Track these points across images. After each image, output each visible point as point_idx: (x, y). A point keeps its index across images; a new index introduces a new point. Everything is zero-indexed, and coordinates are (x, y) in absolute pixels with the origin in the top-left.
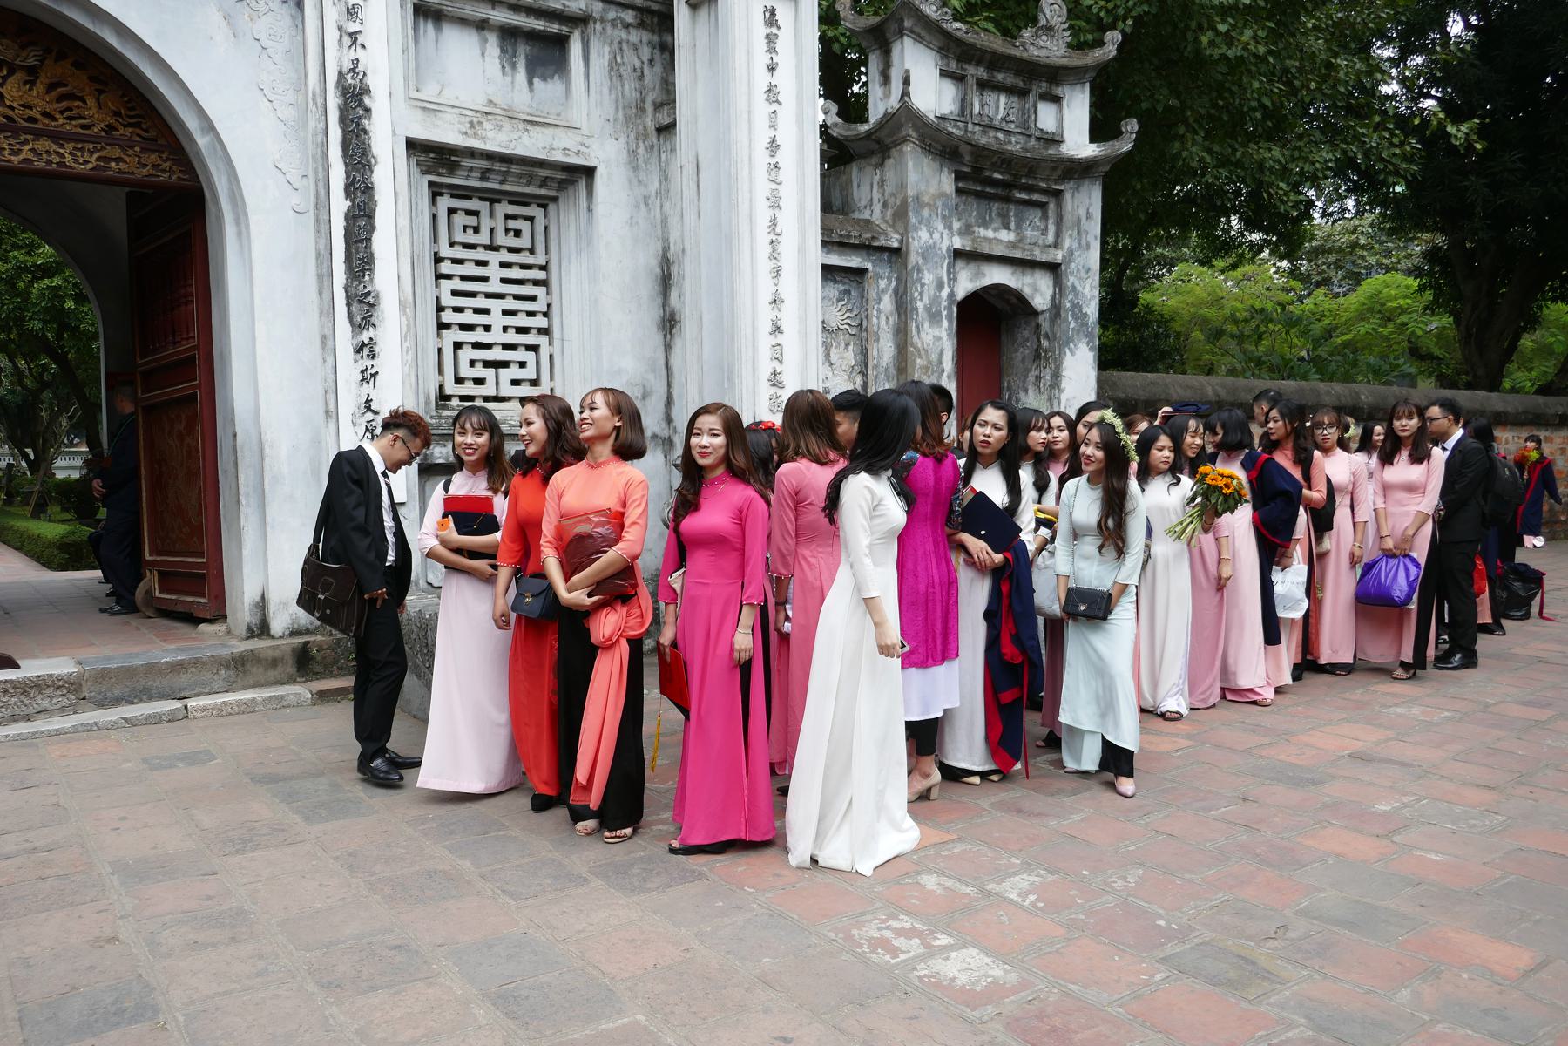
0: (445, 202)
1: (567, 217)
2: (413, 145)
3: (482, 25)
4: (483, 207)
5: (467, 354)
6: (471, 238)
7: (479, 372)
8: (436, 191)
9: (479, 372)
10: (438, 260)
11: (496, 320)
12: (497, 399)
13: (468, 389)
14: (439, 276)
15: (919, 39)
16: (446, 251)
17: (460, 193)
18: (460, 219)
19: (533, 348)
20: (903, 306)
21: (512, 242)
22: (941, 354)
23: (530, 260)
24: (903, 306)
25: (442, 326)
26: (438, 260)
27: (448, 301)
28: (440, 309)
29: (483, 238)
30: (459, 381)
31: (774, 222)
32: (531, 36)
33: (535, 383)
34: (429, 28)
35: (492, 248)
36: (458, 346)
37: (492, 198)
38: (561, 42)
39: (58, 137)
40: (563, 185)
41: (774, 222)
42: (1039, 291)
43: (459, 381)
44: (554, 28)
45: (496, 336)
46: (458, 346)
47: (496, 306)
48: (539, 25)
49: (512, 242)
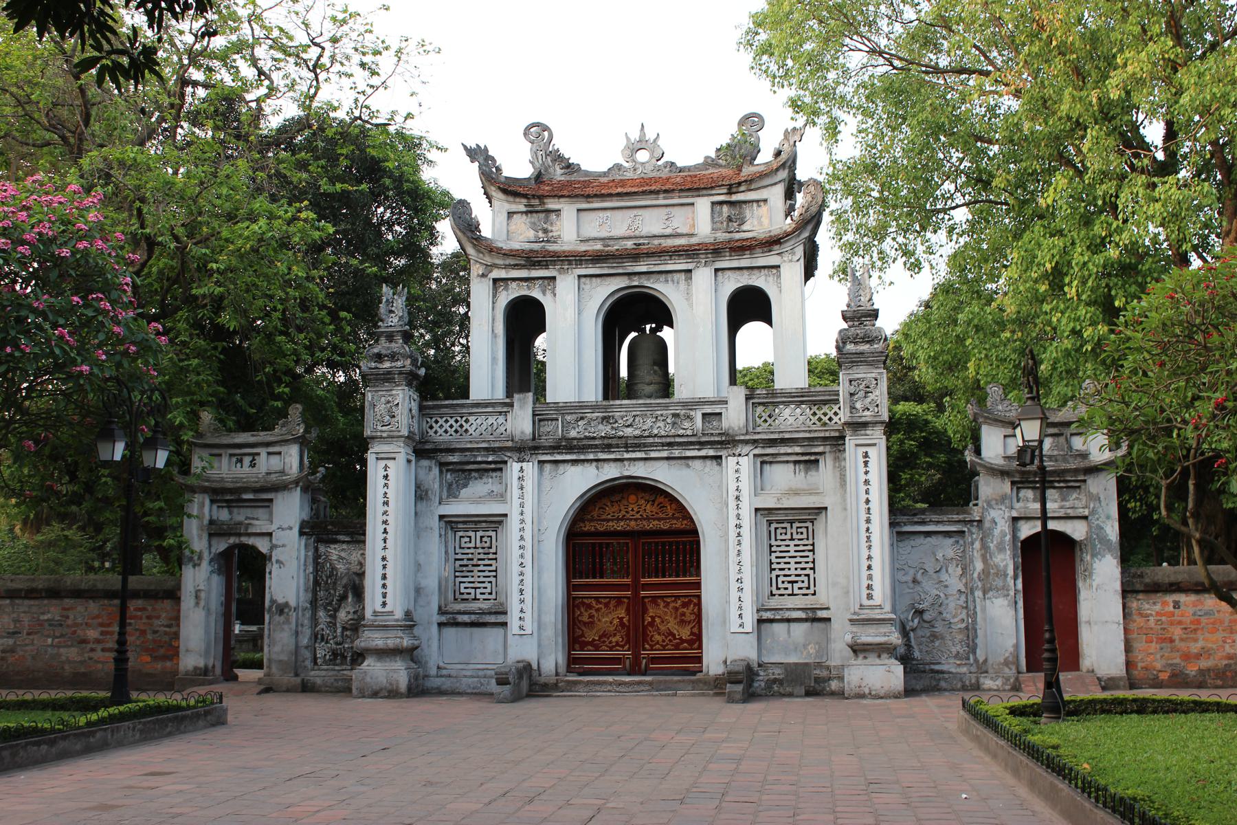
0: (774, 526)
1: (819, 525)
2: (757, 510)
3: (787, 462)
4: (788, 526)
5: (780, 580)
6: (783, 537)
7: (786, 585)
8: (770, 523)
9: (786, 585)
10: (771, 546)
11: (793, 566)
12: (793, 595)
13: (782, 591)
14: (771, 552)
15: (989, 424)
16: (773, 542)
17: (779, 522)
18: (779, 531)
19: (808, 575)
20: (984, 547)
21: (800, 536)
22: (1006, 566)
23: (805, 542)
24: (984, 547)
25: (772, 570)
26: (771, 546)
27: (774, 560)
28: (771, 563)
29: (789, 536)
30: (778, 589)
31: (868, 530)
32: (806, 462)
33: (808, 588)
34: (767, 467)
35: (792, 539)
36: (778, 576)
37: (791, 522)
38: (817, 461)
39: (659, 519)
40: (817, 514)
41: (868, 530)
42: (1077, 531)
43: (778, 589)
44: (813, 458)
45: (793, 572)
46: (778, 576)
47: (792, 561)
48: (806, 458)
49: (800, 536)
